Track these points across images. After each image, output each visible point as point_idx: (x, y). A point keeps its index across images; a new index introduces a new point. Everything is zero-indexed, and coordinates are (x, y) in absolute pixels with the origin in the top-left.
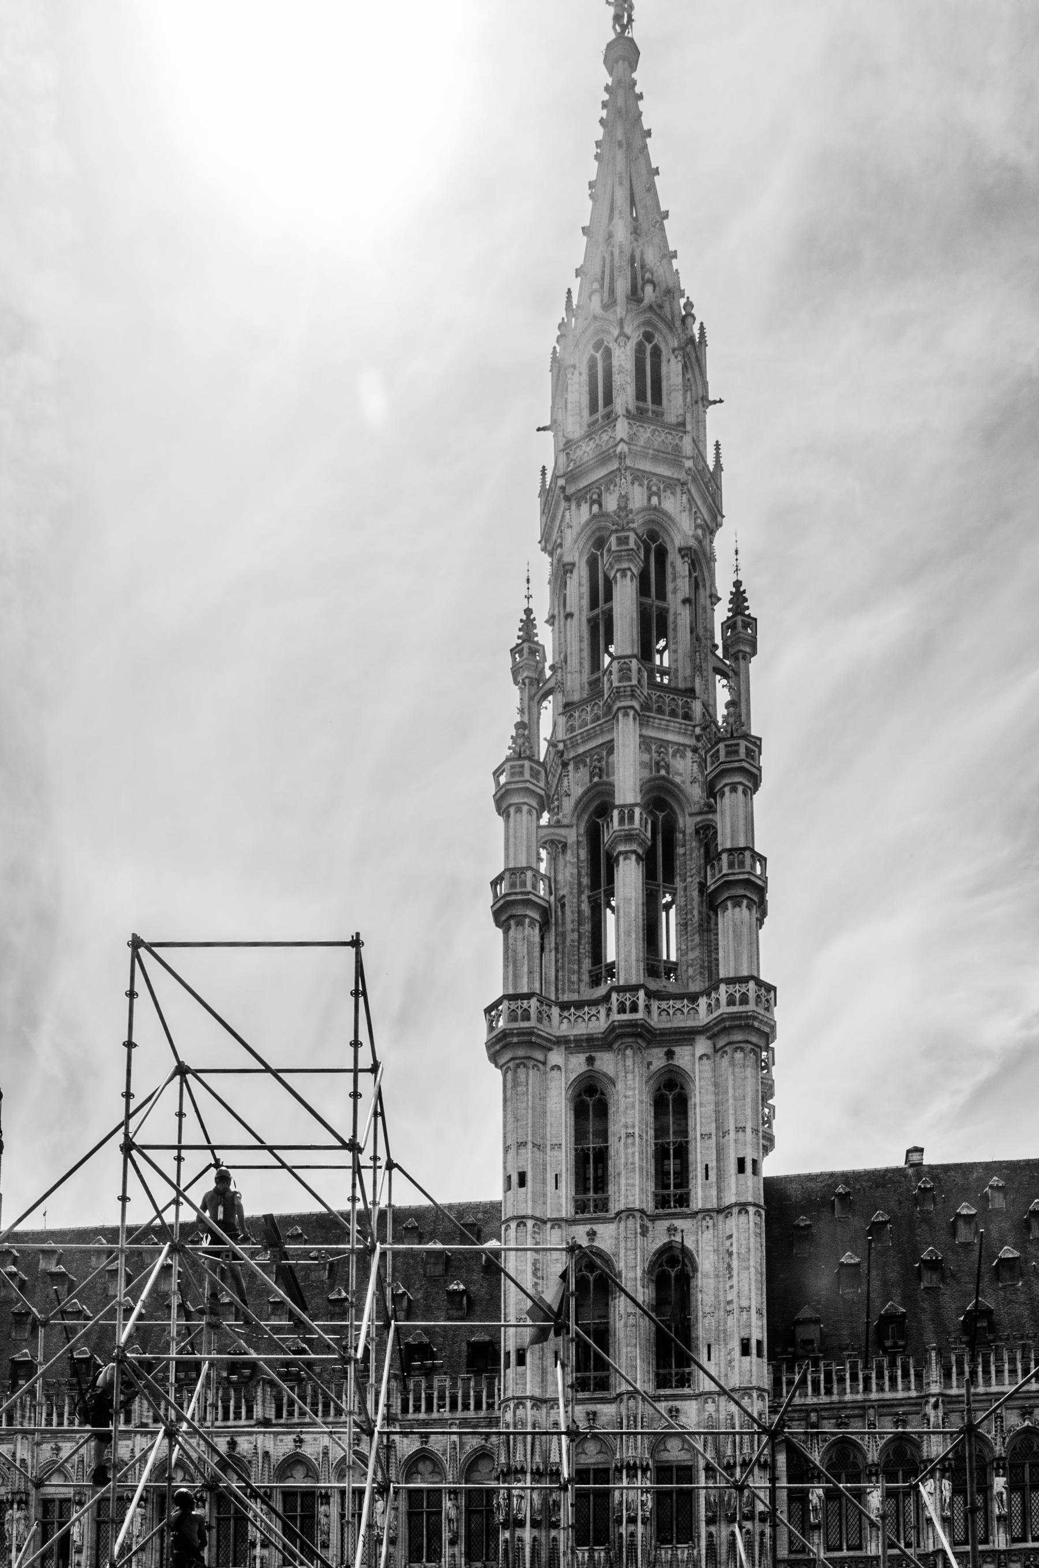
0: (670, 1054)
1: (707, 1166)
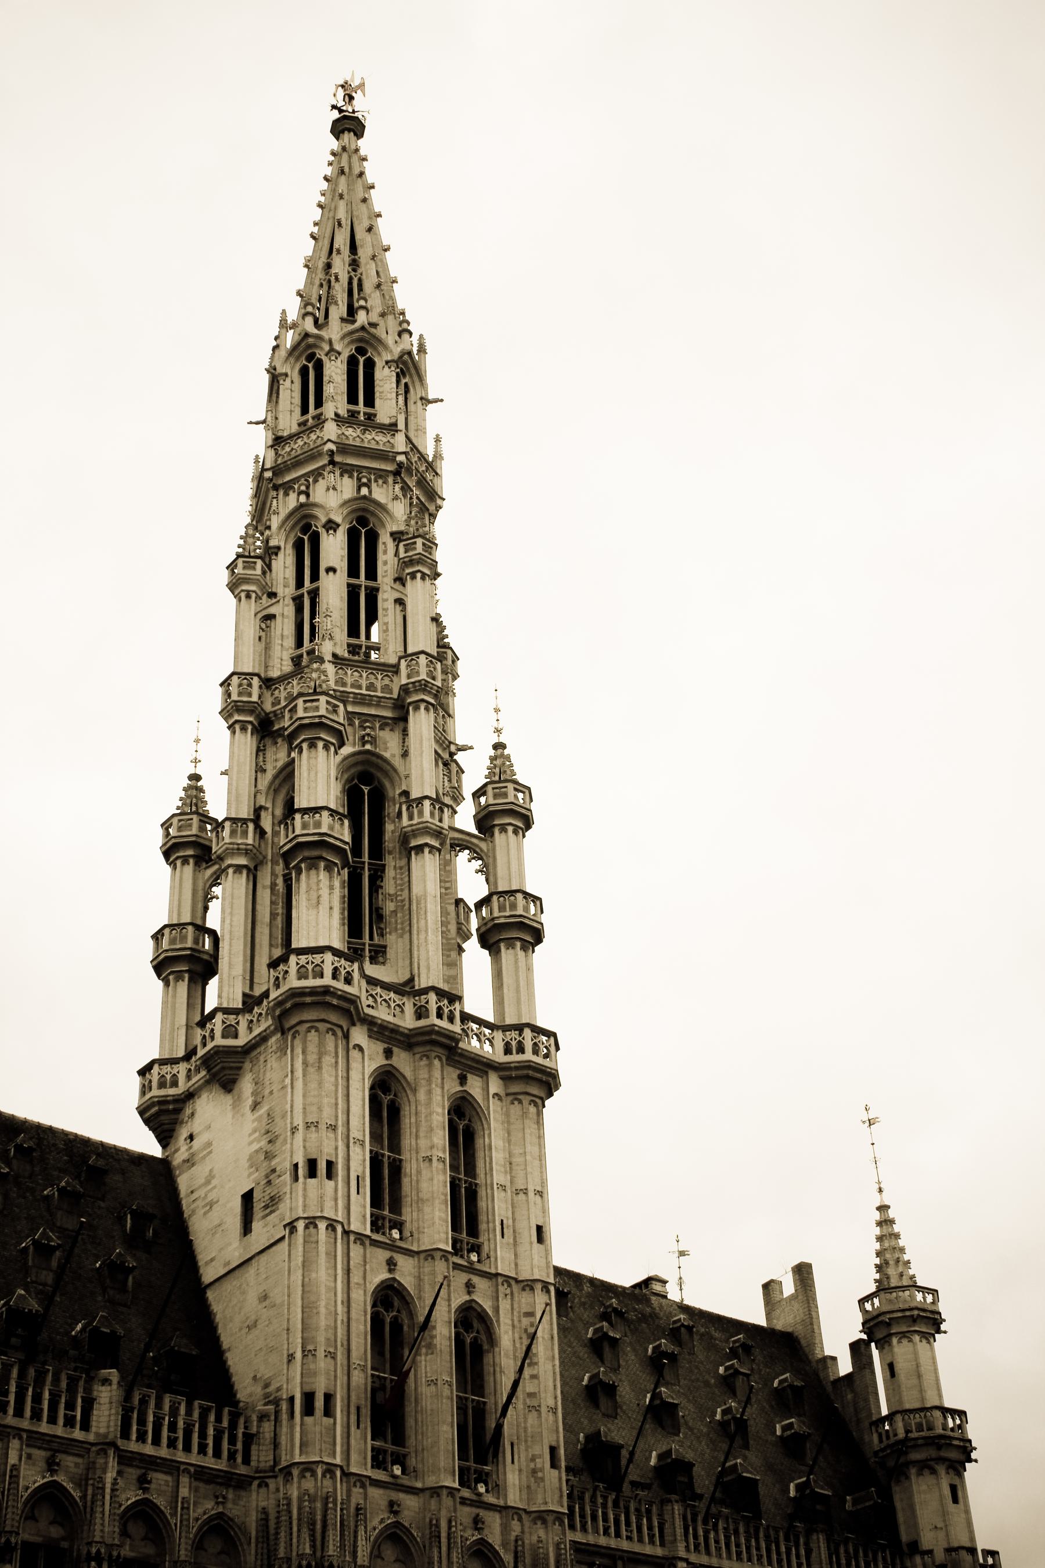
0: (463, 1080)
1: (502, 1221)
